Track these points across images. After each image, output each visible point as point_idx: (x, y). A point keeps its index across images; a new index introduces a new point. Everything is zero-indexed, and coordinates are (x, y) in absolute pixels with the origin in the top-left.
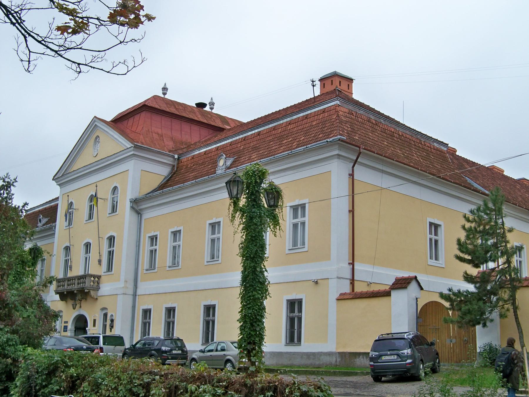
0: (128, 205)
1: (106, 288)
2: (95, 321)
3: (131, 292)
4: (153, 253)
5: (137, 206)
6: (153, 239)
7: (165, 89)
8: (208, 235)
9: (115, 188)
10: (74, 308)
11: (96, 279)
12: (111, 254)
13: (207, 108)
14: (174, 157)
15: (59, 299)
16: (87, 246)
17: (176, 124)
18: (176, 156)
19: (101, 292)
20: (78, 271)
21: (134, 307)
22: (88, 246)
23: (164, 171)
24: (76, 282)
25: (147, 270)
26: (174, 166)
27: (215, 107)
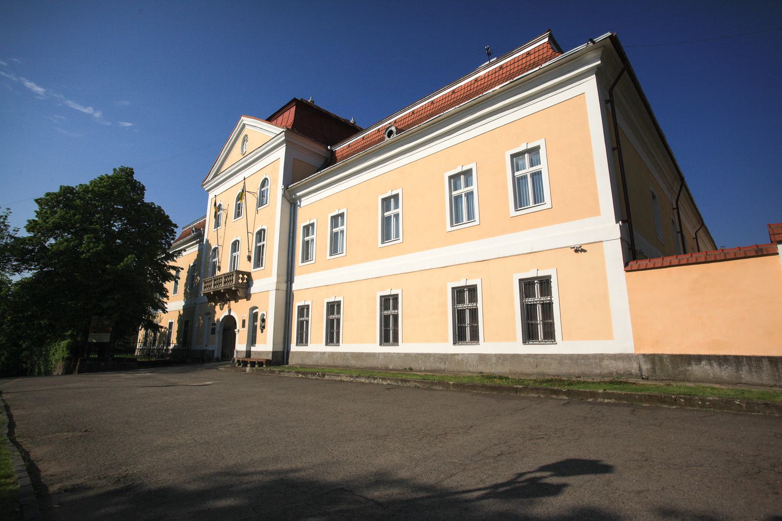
11: (246, 276)
24: (223, 280)
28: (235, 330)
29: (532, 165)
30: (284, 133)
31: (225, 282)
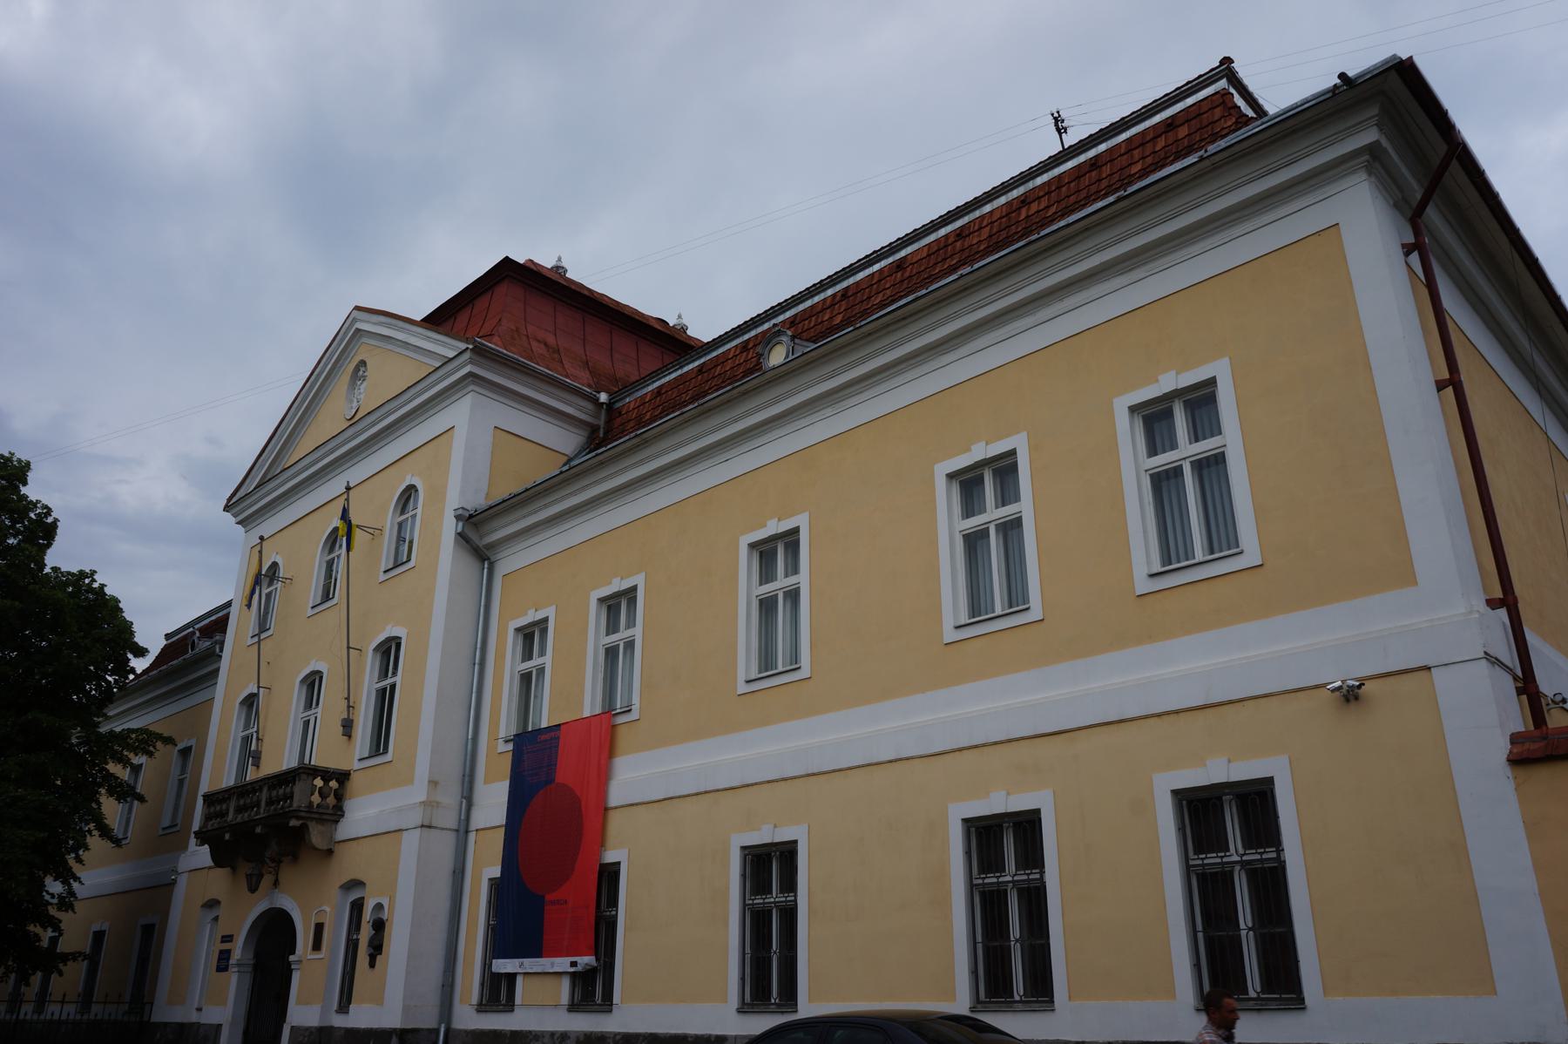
0: (450, 527)
1: (364, 813)
2: (319, 928)
3: (449, 819)
5: (479, 534)
6: (531, 636)
8: (746, 587)
9: (410, 491)
10: (253, 890)
11: (333, 784)
15: (210, 863)
16: (312, 685)
19: (345, 829)
21: (458, 874)
22: (313, 682)
24: (264, 795)
26: (594, 429)
28: (292, 958)
29: (1196, 437)
31: (270, 802)
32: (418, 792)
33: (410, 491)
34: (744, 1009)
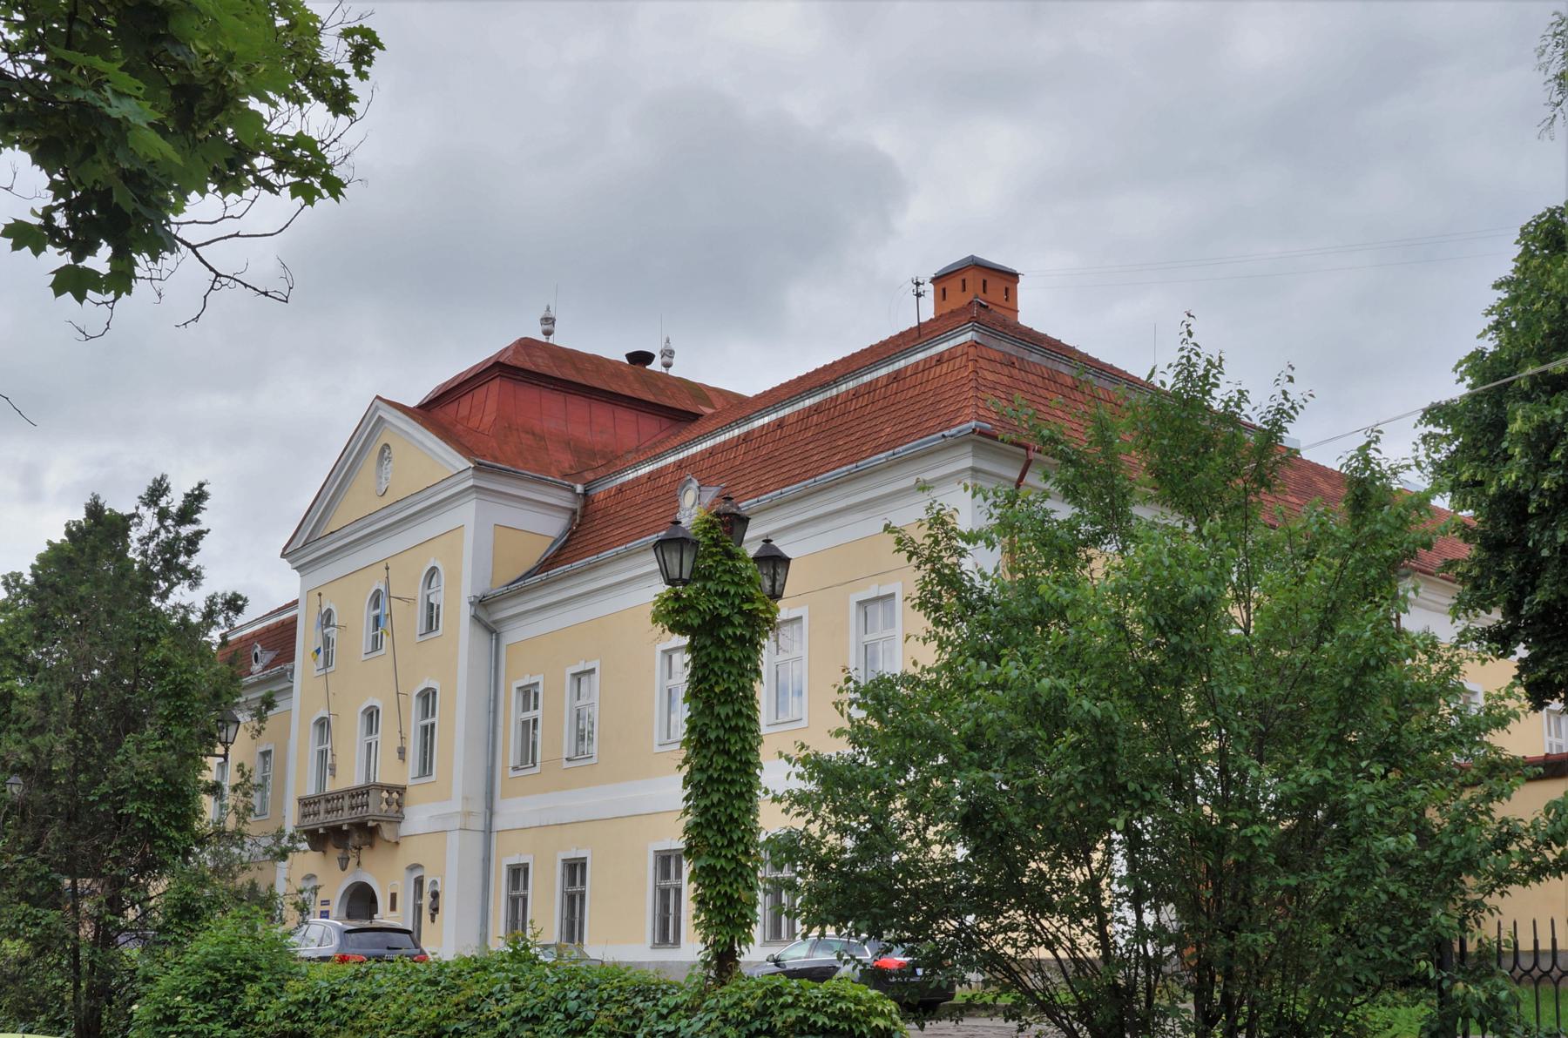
0: (466, 612)
1: (418, 818)
2: (394, 896)
3: (478, 823)
4: (529, 727)
6: (529, 695)
7: (548, 321)
9: (433, 571)
10: (343, 869)
11: (395, 795)
12: (428, 732)
13: (656, 366)
14: (573, 490)
17: (578, 406)
18: (579, 488)
19: (406, 828)
20: (350, 776)
21: (487, 860)
22: (372, 715)
23: (551, 526)
24: (347, 802)
25: (515, 769)
26: (574, 512)
27: (675, 361)
30: (470, 472)
32: (456, 805)
33: (433, 571)
34: (654, 946)
